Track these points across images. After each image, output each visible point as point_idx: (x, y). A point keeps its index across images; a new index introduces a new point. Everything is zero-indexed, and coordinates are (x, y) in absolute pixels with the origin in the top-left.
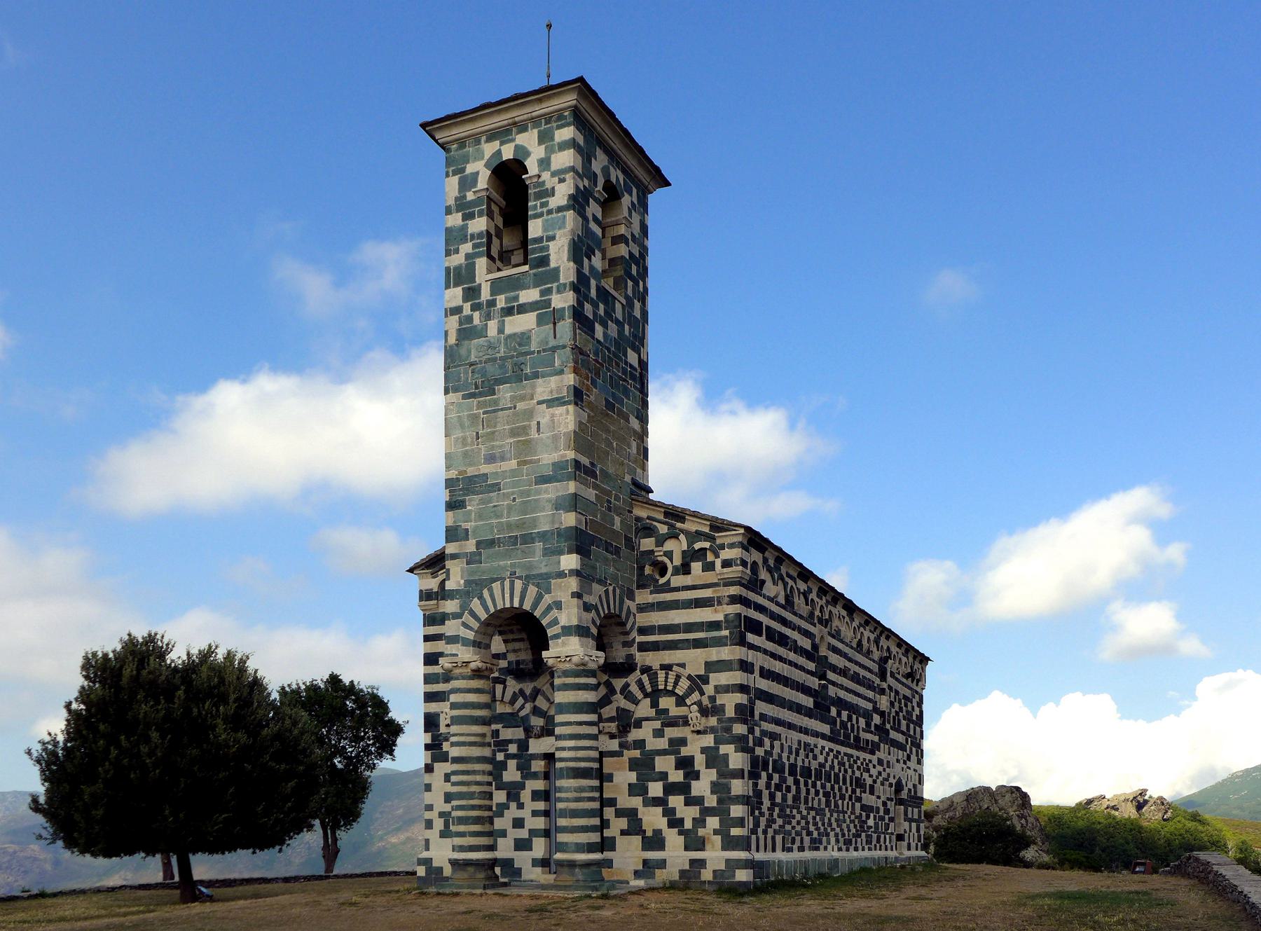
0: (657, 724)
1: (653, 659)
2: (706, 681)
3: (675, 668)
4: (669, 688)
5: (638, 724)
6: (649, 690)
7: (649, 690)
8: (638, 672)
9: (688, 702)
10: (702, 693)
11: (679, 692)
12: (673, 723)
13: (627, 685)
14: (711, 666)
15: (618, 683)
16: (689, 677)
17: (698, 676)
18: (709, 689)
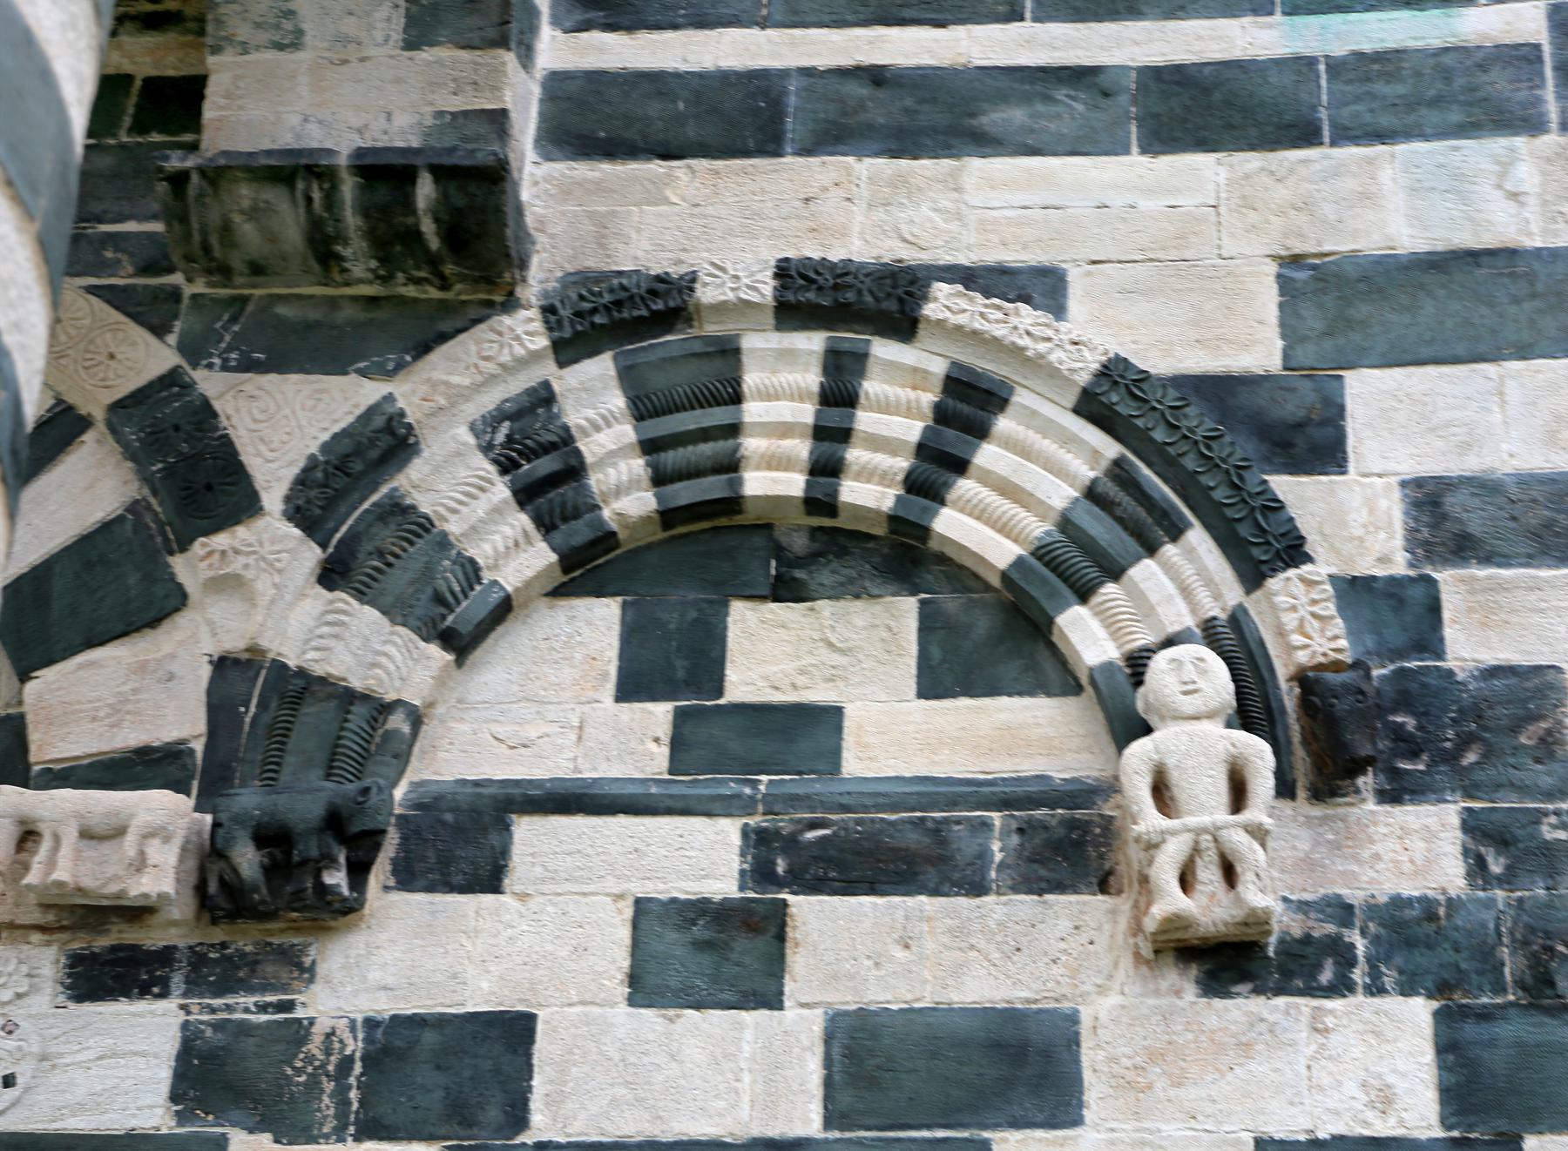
0: (704, 858)
1: (719, 228)
2: (1318, 445)
3: (943, 302)
4: (869, 490)
5: (464, 846)
6: (623, 490)
7: (623, 490)
8: (523, 331)
9: (1088, 635)
10: (1264, 547)
11: (981, 527)
12: (901, 850)
13: (386, 442)
14: (1352, 304)
15: (282, 423)
16: (1112, 398)
17: (1217, 391)
18: (1352, 518)
